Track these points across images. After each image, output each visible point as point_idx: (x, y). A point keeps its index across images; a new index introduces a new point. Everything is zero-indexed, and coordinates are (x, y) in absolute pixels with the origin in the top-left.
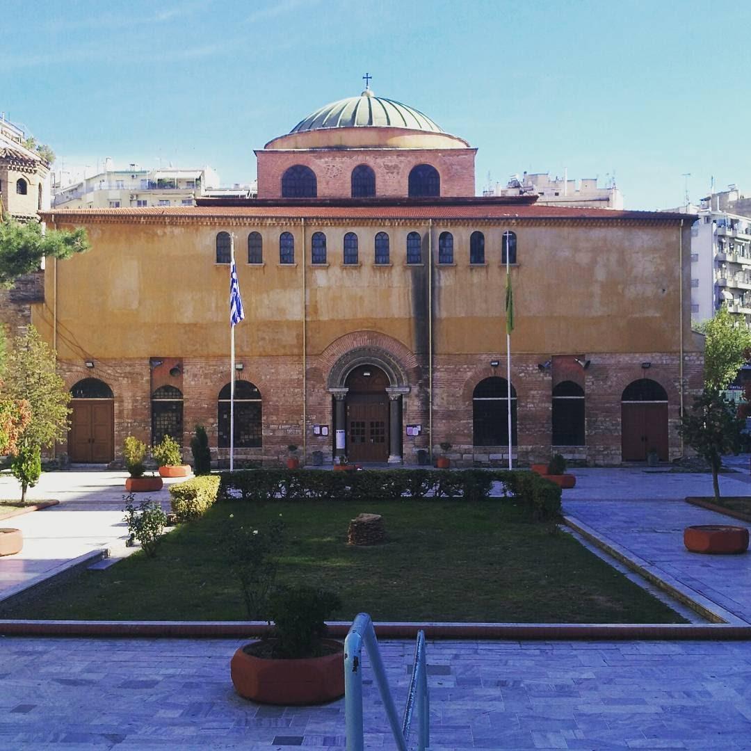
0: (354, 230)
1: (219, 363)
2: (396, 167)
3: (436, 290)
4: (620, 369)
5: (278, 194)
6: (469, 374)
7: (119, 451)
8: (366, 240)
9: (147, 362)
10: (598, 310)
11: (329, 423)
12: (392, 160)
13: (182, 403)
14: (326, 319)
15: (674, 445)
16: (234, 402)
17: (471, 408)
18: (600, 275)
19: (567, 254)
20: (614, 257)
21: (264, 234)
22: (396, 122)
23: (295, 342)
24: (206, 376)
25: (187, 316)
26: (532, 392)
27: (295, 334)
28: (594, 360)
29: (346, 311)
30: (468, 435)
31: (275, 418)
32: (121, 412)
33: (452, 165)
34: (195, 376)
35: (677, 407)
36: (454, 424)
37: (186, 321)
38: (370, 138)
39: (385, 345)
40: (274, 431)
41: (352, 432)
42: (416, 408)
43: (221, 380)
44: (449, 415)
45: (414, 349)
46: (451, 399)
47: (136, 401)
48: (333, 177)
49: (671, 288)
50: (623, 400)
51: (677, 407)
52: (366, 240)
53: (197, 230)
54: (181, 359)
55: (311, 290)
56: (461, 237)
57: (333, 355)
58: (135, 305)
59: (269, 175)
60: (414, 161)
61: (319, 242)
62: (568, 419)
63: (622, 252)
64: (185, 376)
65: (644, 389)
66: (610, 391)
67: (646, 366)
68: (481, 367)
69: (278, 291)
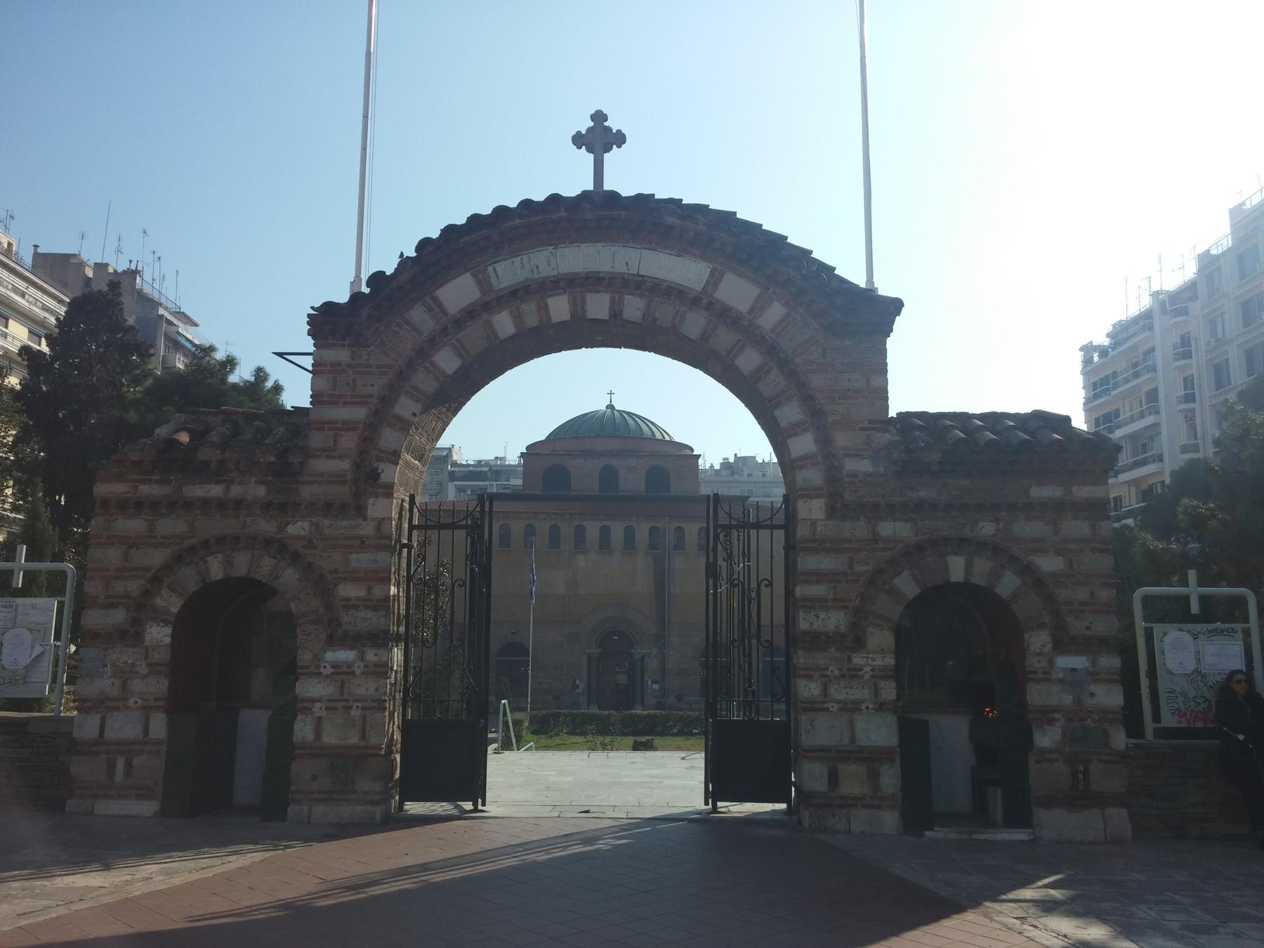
0: (608, 523)
8: (617, 531)
52: (617, 531)
61: (580, 530)
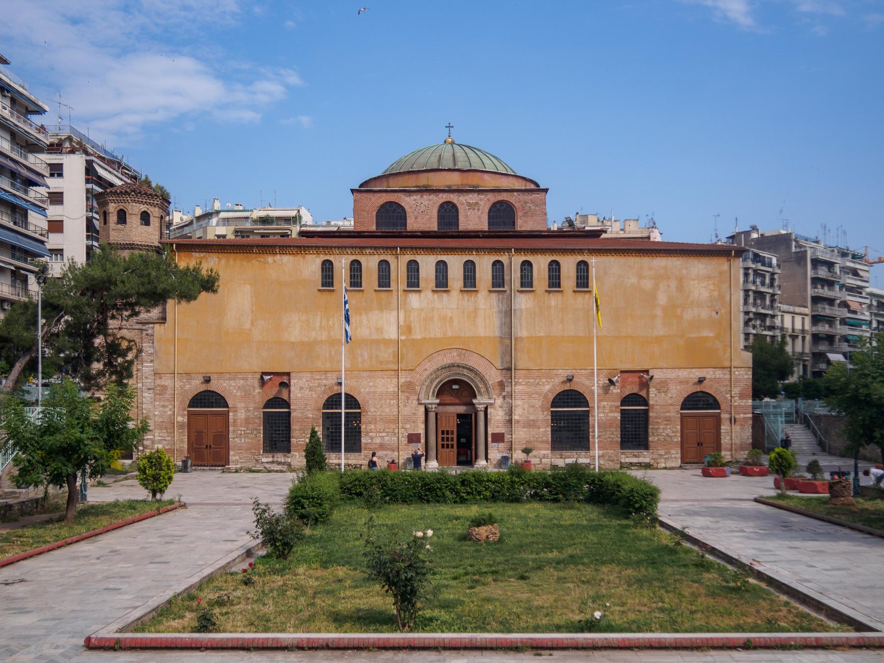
1: (323, 377)
2: (477, 203)
3: (518, 312)
4: (680, 382)
5: (373, 228)
6: (548, 387)
7: (234, 455)
8: (455, 264)
9: (259, 376)
10: (660, 330)
11: (421, 431)
12: (472, 198)
13: (289, 413)
14: (419, 337)
15: (726, 450)
16: (346, 413)
17: (549, 417)
18: (662, 299)
19: (633, 281)
20: (673, 284)
21: (362, 259)
22: (477, 165)
23: (391, 359)
24: (311, 389)
25: (295, 334)
26: (603, 403)
27: (391, 350)
28: (657, 374)
29: (436, 331)
30: (546, 442)
31: (373, 427)
32: (235, 421)
33: (526, 203)
34: (301, 388)
35: (728, 416)
36: (534, 432)
37: (293, 339)
38: (454, 180)
39: (473, 361)
40: (372, 438)
41: (443, 439)
42: (499, 418)
43: (325, 392)
44: (530, 424)
45: (499, 365)
46: (531, 410)
47: (250, 411)
48: (422, 214)
49: (723, 311)
50: (682, 409)
51: (728, 416)
53: (304, 257)
54: (288, 374)
55: (405, 311)
56: (541, 264)
57: (426, 370)
58: (247, 326)
59: (365, 211)
60: (493, 198)
61: (413, 267)
62: (635, 430)
63: (680, 280)
64: (292, 388)
65: (700, 401)
66: (670, 402)
67: (701, 381)
68: (558, 381)
69: (376, 312)
